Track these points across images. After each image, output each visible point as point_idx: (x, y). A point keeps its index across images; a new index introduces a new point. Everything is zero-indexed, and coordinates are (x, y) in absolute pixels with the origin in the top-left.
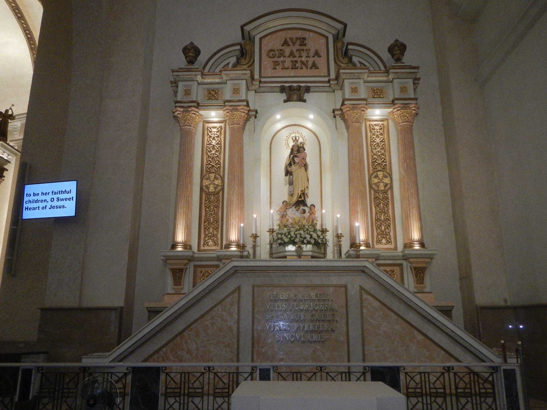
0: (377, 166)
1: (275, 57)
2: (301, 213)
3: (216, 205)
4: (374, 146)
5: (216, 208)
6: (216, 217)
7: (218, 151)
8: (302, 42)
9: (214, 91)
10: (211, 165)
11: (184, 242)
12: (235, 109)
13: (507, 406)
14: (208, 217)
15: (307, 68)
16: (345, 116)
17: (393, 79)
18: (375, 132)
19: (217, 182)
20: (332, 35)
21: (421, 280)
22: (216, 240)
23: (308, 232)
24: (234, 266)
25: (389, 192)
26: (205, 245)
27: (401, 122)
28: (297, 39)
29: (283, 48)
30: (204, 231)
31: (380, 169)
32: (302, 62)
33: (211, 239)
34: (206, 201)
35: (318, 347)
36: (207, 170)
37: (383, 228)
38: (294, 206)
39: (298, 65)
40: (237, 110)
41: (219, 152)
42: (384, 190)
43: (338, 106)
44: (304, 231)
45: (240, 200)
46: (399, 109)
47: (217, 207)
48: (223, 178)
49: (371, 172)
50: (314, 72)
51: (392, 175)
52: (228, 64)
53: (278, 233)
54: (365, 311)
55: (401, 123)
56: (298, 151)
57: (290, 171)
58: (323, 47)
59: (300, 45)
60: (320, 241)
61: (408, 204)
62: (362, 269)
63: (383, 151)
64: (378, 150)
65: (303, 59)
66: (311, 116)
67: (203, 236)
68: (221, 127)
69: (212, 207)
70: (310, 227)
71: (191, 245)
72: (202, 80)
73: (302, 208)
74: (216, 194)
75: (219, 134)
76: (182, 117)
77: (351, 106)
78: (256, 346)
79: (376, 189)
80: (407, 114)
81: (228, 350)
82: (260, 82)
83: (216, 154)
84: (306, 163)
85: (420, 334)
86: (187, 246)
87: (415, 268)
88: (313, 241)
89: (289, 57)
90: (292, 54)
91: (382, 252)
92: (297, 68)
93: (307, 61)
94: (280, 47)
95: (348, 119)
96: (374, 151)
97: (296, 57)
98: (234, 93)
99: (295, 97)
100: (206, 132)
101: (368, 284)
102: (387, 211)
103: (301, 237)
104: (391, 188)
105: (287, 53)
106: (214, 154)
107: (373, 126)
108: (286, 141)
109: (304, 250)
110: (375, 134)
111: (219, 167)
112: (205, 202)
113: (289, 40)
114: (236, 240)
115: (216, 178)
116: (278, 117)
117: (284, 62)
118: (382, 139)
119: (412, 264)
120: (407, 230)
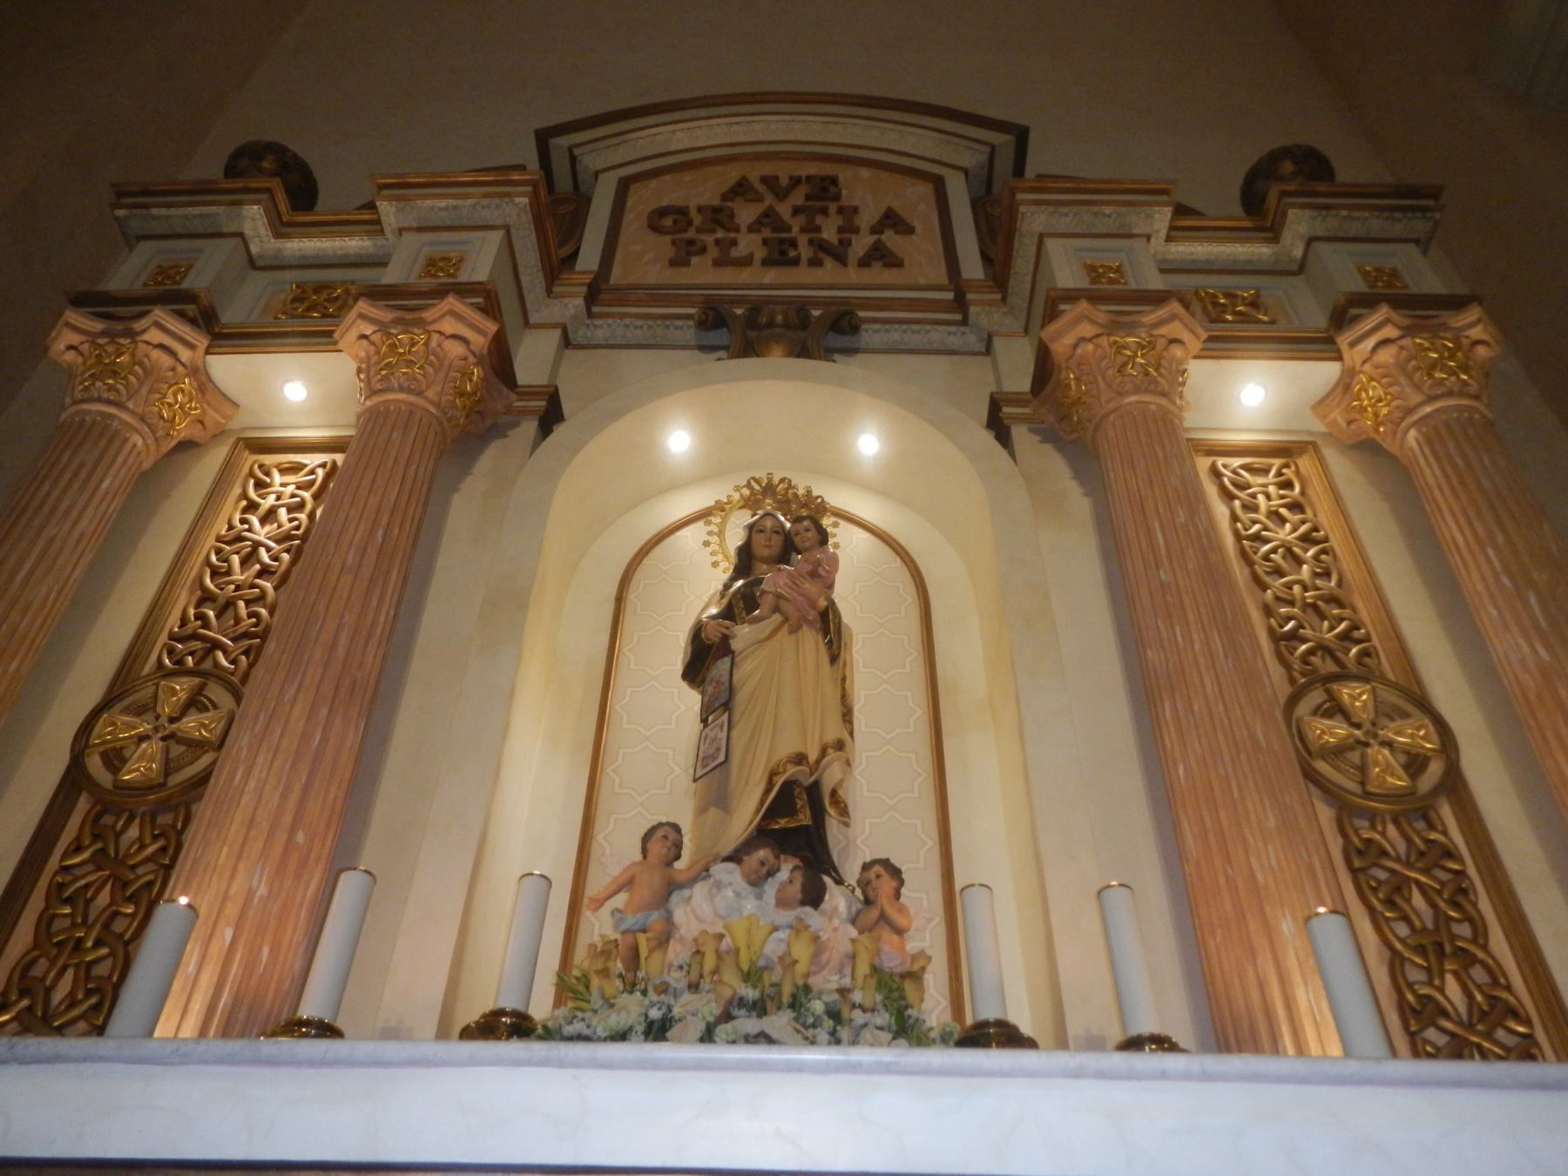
6: (102, 970)
8: (825, 190)
17: (1311, 241)
18: (1254, 496)
20: (962, 176)
25: (1446, 812)
40: (421, 323)
42: (1410, 794)
46: (1390, 332)
55: (1421, 404)
72: (273, 244)
79: (1352, 786)
83: (253, 586)
84: (832, 603)
104: (1454, 785)
110: (1255, 509)
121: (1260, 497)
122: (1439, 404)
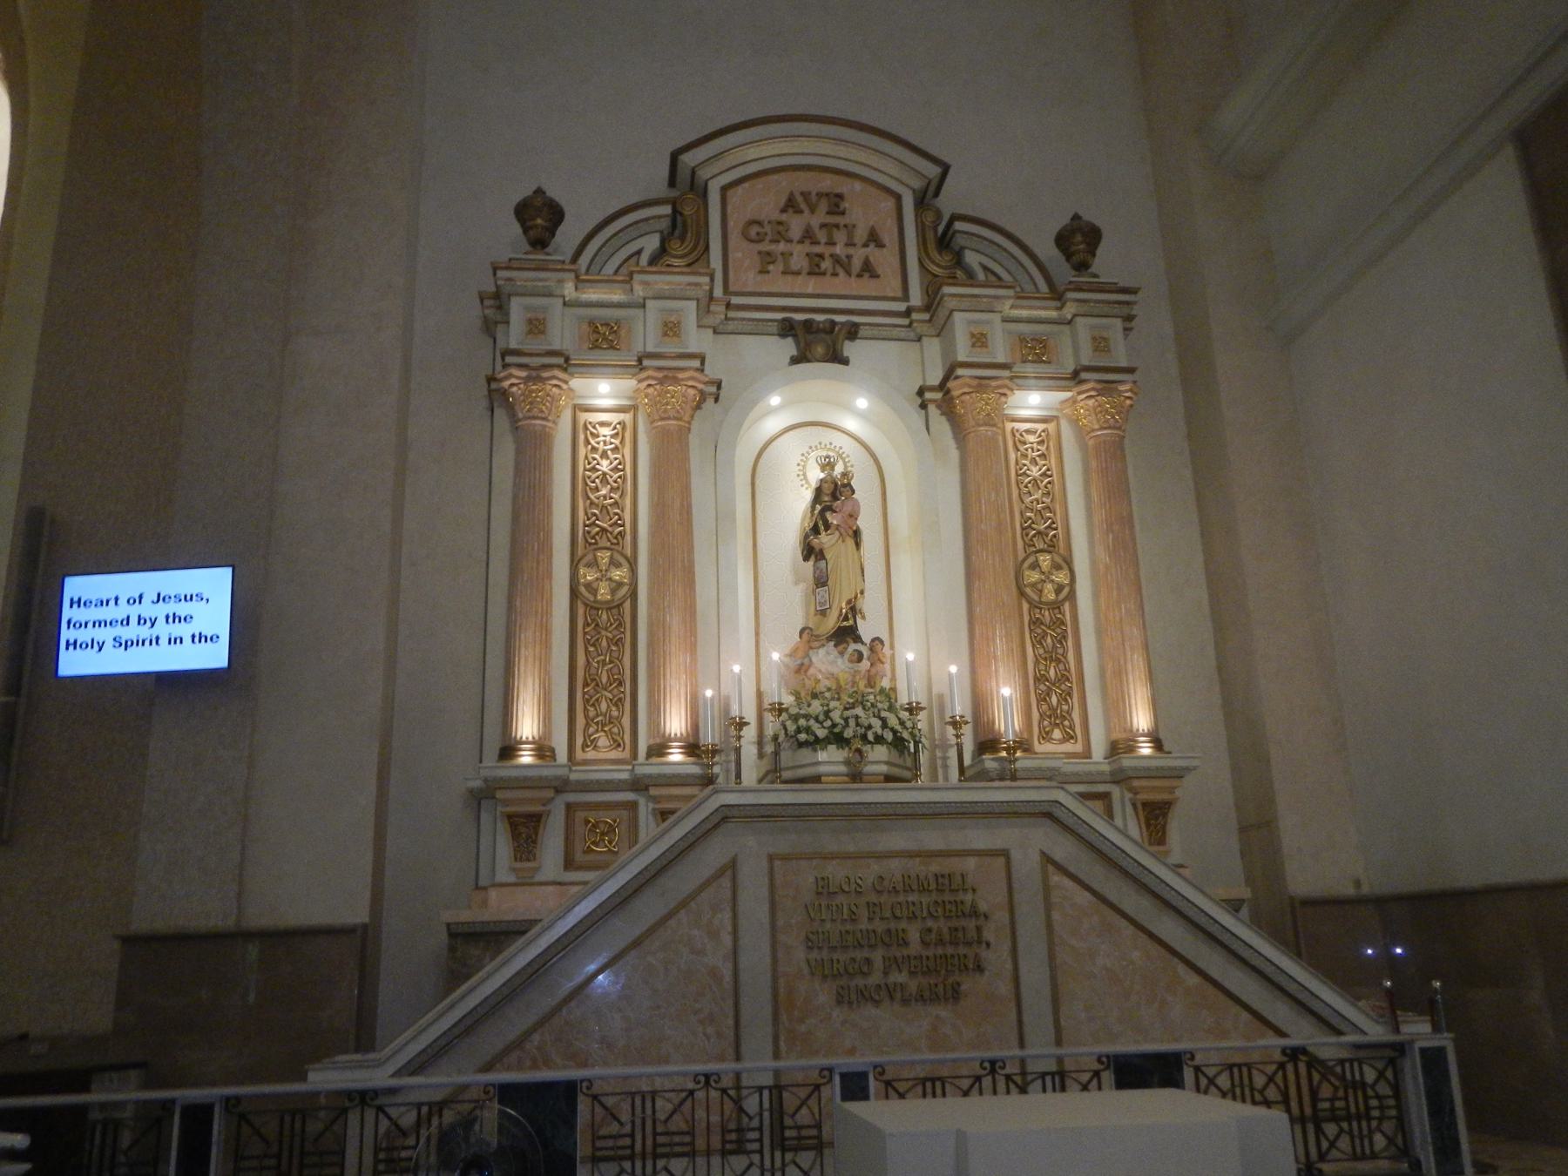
0: (1034, 539)
1: (763, 240)
2: (851, 661)
3: (614, 637)
4: (1026, 487)
5: (616, 644)
7: (618, 488)
8: (836, 203)
9: (607, 325)
10: (598, 526)
11: (537, 738)
12: (669, 377)
13: (1432, 1138)
14: (593, 671)
15: (850, 275)
16: (955, 407)
17: (1075, 316)
18: (1027, 450)
19: (617, 574)
20: (911, 192)
21: (1160, 834)
22: (619, 733)
23: (876, 711)
24: (722, 806)
25: (1067, 606)
26: (588, 746)
27: (1097, 427)
28: (820, 195)
29: (784, 217)
30: (585, 707)
31: (1041, 546)
32: (836, 260)
33: (605, 731)
34: (588, 625)
35: (943, 1014)
36: (587, 541)
37: (1054, 700)
38: (833, 643)
39: (826, 264)
40: (676, 381)
41: (619, 493)
43: (935, 378)
44: (864, 709)
45: (688, 625)
47: (619, 642)
48: (632, 561)
49: (1021, 555)
50: (867, 286)
51: (1072, 561)
52: (639, 252)
53: (795, 718)
54: (1056, 916)
55: (1098, 430)
56: (835, 497)
57: (817, 548)
58: (889, 221)
59: (828, 213)
60: (906, 735)
61: (1120, 639)
62: (1046, 808)
63: (1049, 500)
64: (1036, 497)
65: (839, 250)
66: (862, 403)
67: (580, 721)
68: (624, 423)
69: (604, 643)
70: (878, 698)
71: (553, 745)
73: (853, 646)
74: (614, 607)
75: (617, 442)
76: (523, 394)
77: (975, 382)
78: (784, 1018)
79: (1036, 598)
80: (1111, 408)
81: (710, 1030)
82: (728, 306)
83: (611, 498)
84: (858, 527)
85: (1189, 970)
86: (543, 750)
87: (1145, 805)
88: (889, 736)
89: (801, 242)
90: (808, 236)
91: (1065, 763)
92: (824, 274)
93: (849, 257)
94: (776, 216)
95: (964, 416)
96: (1028, 500)
97: (819, 243)
98: (665, 334)
99: (820, 350)
100: (582, 437)
101: (1064, 848)
102: (1063, 655)
103: (858, 725)
104: (1072, 596)
105: (796, 232)
106: (605, 497)
107: (1021, 435)
108: (801, 468)
109: (870, 759)
111: (620, 532)
112: (584, 629)
113: (800, 199)
114: (681, 734)
115: (614, 563)
116: (775, 400)
117: (786, 256)
118: (1044, 468)
119: (1136, 794)
120: (1116, 707)
121: (1030, 450)
122: (1105, 432)
